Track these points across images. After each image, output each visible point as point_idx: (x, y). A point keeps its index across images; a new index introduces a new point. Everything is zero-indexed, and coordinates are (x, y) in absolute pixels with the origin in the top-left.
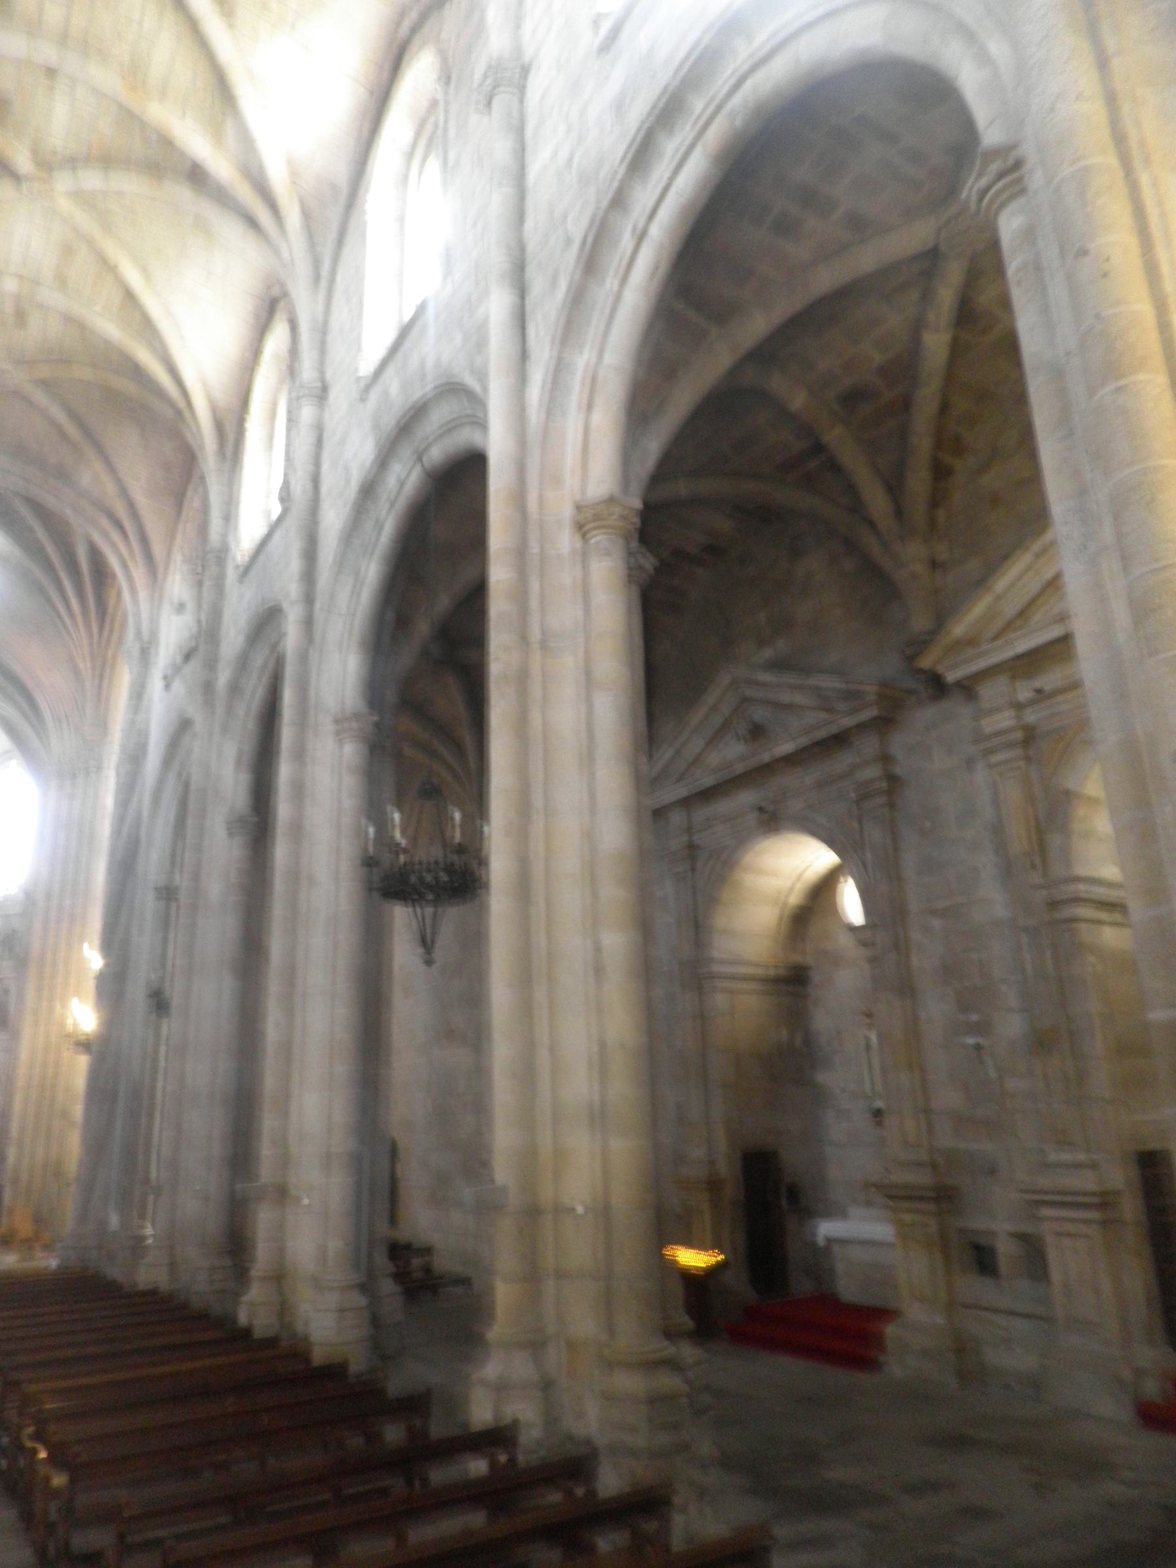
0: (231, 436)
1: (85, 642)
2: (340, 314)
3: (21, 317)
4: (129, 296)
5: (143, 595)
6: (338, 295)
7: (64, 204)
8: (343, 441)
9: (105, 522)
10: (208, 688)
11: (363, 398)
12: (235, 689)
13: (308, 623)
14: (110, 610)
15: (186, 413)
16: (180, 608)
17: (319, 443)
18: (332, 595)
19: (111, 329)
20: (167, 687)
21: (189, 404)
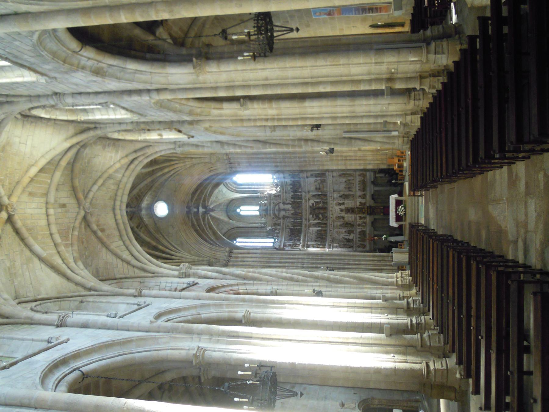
0: (86, 126)
1: (178, 165)
2: (22, 91)
3: (64, 206)
4: (41, 170)
5: (157, 149)
6: (12, 93)
7: (14, 199)
8: (77, 85)
9: (132, 166)
10: (191, 123)
11: (55, 78)
12: (190, 113)
13: (158, 90)
14: (165, 158)
15: (82, 144)
16: (160, 135)
17: (80, 93)
18: (145, 82)
19: (58, 175)
20: (193, 137)
21: (78, 143)
